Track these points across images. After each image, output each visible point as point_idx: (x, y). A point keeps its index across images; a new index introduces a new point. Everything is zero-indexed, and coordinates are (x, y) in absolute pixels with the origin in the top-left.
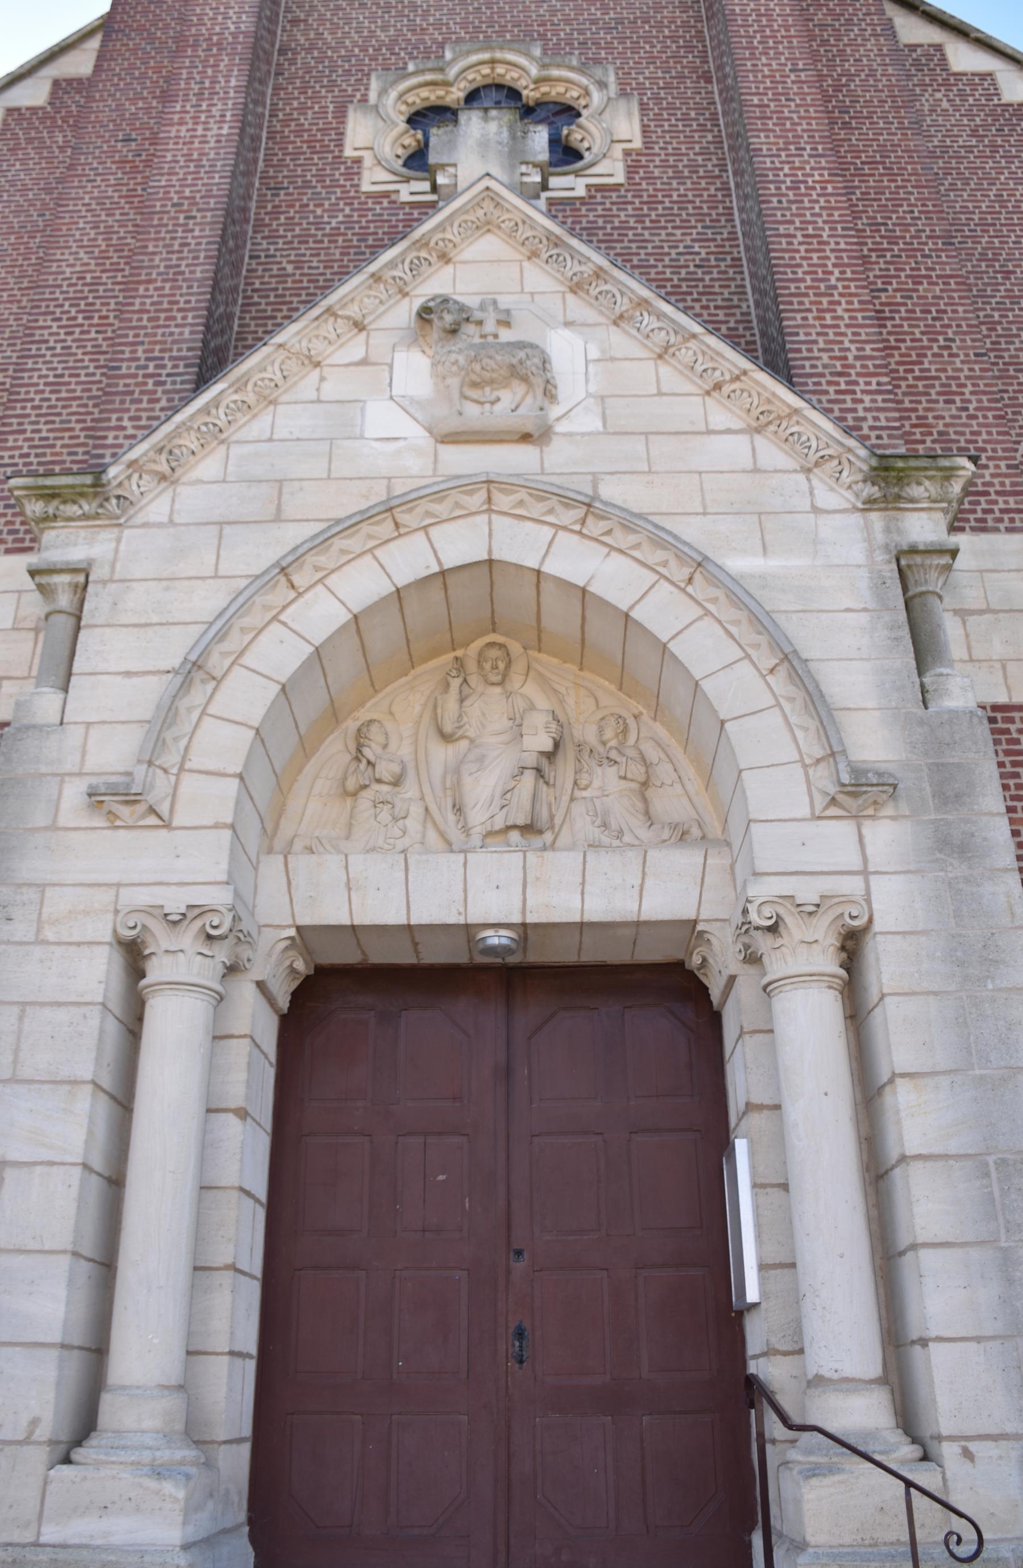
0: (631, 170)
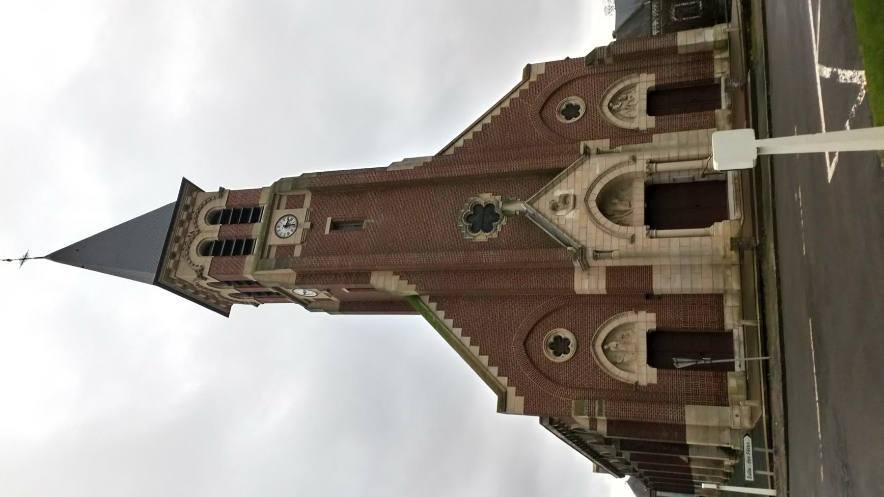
0: (497, 194)
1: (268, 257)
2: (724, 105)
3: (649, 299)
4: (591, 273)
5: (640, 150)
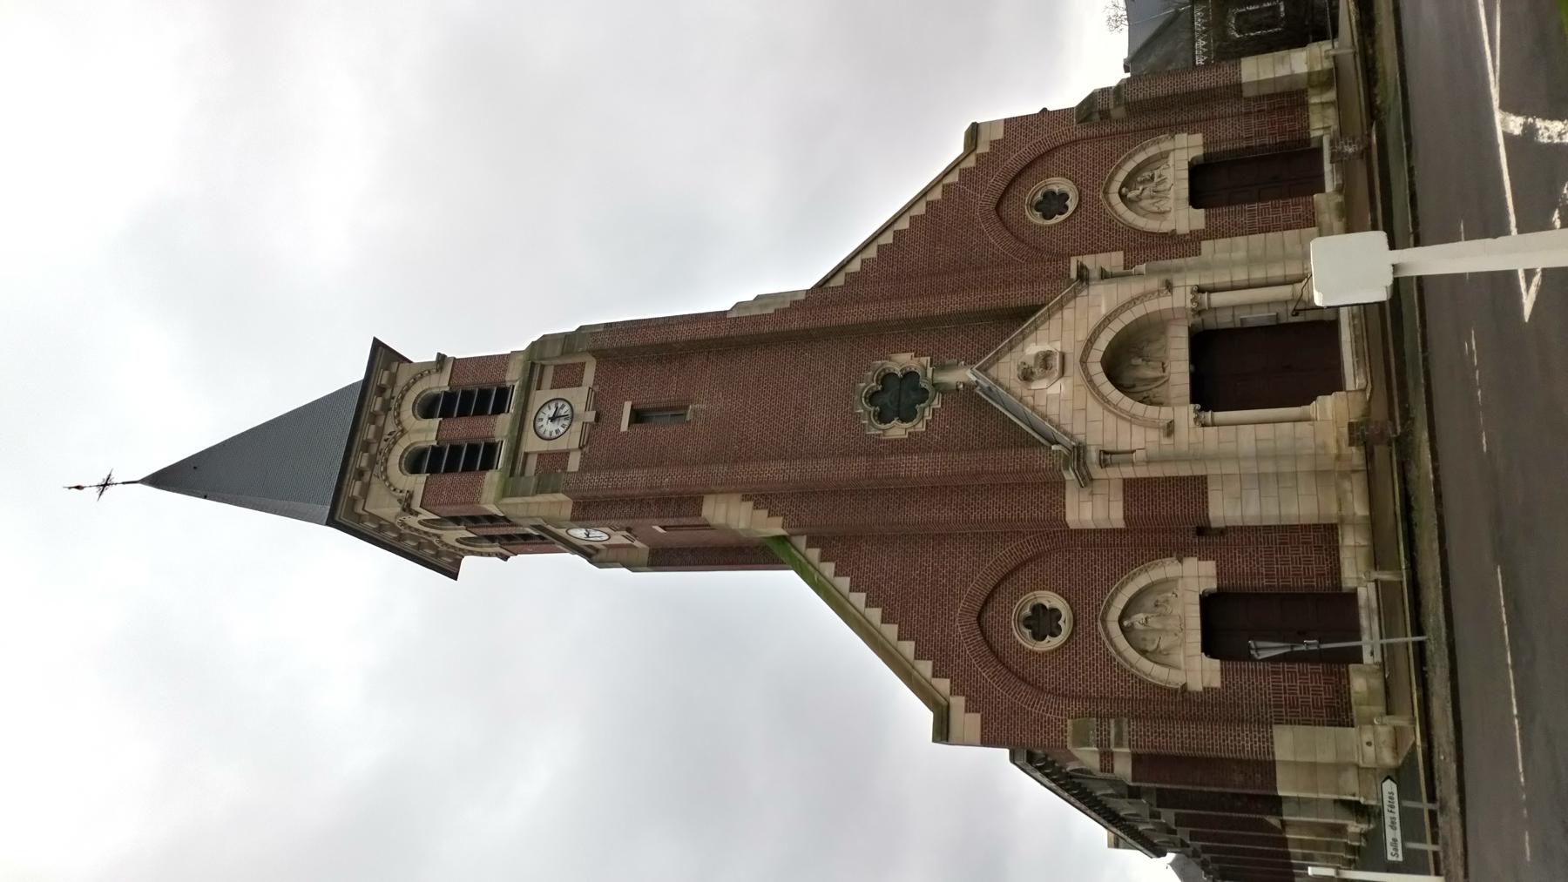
1: (523, 474)
2: (1330, 186)
3: (1204, 536)
4: (1098, 490)
5: (1179, 270)
